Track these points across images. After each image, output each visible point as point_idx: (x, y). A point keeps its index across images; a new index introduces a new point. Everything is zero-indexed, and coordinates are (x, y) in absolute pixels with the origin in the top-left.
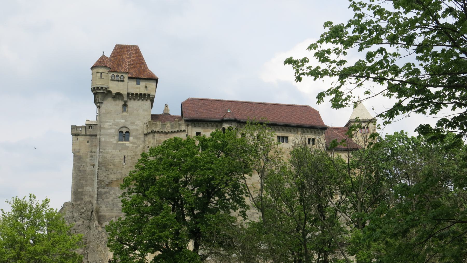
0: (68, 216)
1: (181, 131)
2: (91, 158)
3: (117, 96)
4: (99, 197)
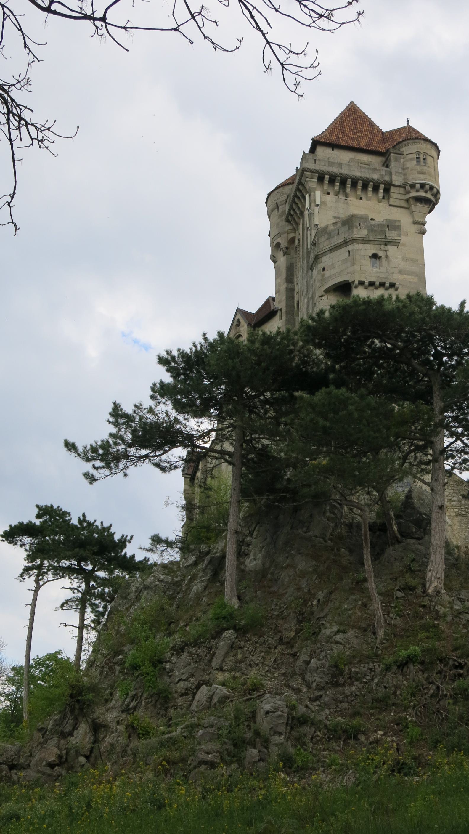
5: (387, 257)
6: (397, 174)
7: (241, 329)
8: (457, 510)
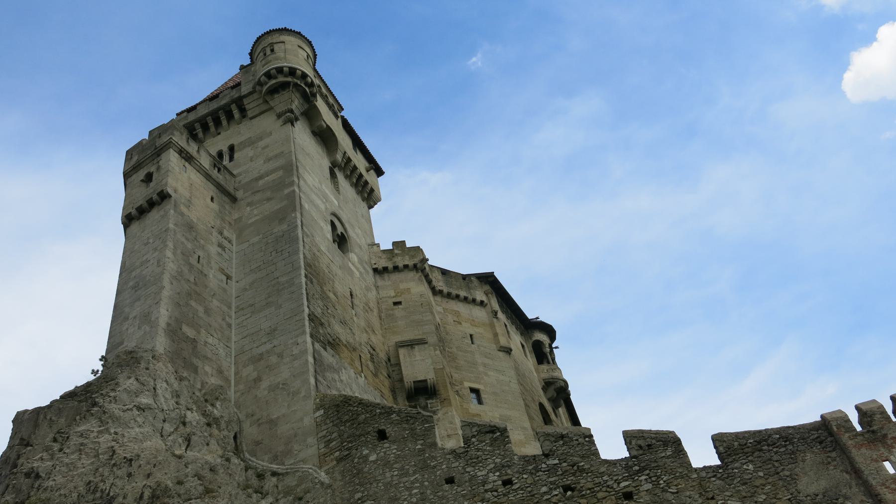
0: (165, 408)
1: (474, 301)
2: (220, 250)
3: (319, 139)
4: (318, 370)
5: (158, 168)
6: (247, 84)
8: (337, 454)
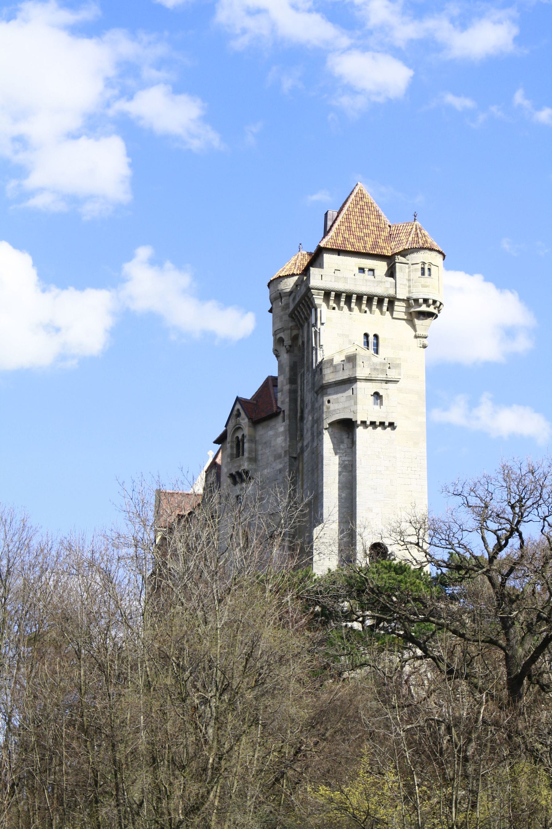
7: (241, 421)
